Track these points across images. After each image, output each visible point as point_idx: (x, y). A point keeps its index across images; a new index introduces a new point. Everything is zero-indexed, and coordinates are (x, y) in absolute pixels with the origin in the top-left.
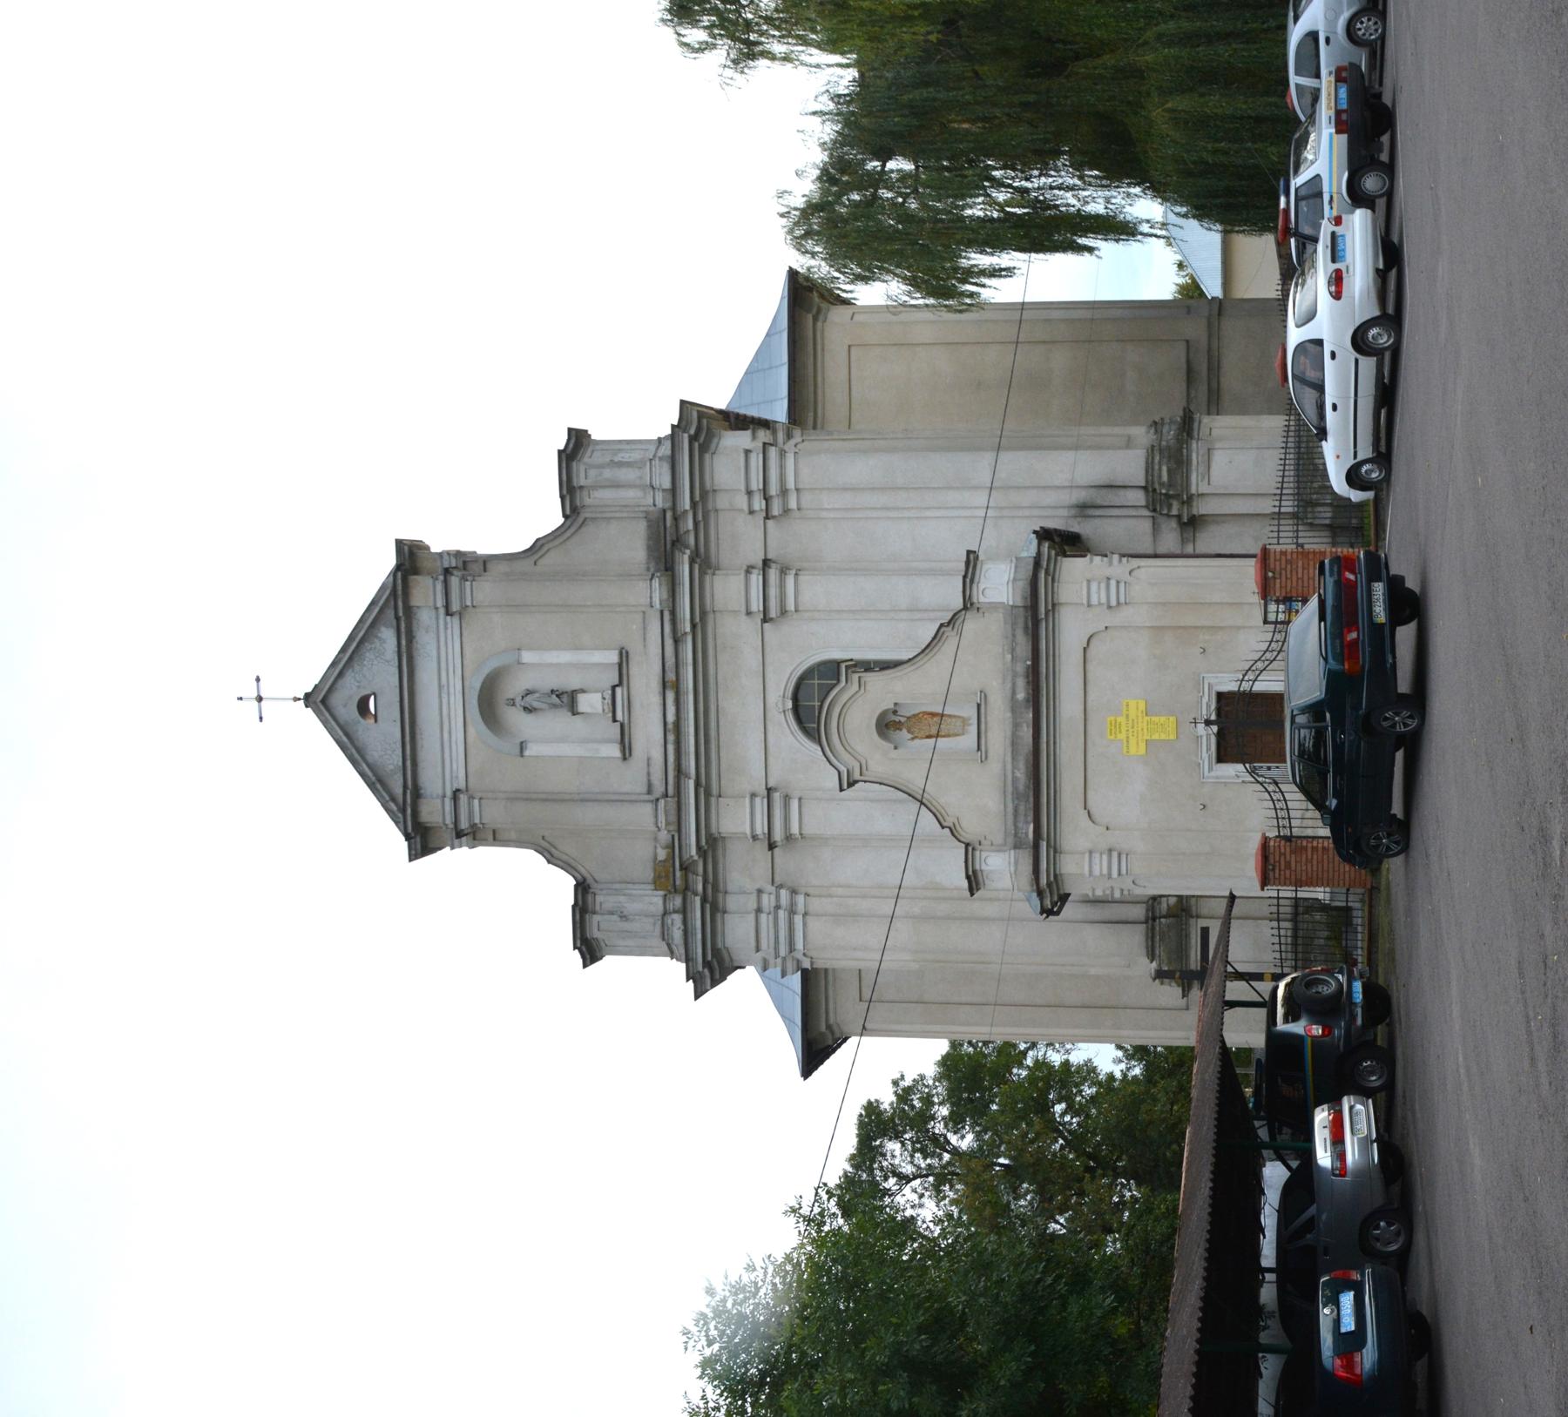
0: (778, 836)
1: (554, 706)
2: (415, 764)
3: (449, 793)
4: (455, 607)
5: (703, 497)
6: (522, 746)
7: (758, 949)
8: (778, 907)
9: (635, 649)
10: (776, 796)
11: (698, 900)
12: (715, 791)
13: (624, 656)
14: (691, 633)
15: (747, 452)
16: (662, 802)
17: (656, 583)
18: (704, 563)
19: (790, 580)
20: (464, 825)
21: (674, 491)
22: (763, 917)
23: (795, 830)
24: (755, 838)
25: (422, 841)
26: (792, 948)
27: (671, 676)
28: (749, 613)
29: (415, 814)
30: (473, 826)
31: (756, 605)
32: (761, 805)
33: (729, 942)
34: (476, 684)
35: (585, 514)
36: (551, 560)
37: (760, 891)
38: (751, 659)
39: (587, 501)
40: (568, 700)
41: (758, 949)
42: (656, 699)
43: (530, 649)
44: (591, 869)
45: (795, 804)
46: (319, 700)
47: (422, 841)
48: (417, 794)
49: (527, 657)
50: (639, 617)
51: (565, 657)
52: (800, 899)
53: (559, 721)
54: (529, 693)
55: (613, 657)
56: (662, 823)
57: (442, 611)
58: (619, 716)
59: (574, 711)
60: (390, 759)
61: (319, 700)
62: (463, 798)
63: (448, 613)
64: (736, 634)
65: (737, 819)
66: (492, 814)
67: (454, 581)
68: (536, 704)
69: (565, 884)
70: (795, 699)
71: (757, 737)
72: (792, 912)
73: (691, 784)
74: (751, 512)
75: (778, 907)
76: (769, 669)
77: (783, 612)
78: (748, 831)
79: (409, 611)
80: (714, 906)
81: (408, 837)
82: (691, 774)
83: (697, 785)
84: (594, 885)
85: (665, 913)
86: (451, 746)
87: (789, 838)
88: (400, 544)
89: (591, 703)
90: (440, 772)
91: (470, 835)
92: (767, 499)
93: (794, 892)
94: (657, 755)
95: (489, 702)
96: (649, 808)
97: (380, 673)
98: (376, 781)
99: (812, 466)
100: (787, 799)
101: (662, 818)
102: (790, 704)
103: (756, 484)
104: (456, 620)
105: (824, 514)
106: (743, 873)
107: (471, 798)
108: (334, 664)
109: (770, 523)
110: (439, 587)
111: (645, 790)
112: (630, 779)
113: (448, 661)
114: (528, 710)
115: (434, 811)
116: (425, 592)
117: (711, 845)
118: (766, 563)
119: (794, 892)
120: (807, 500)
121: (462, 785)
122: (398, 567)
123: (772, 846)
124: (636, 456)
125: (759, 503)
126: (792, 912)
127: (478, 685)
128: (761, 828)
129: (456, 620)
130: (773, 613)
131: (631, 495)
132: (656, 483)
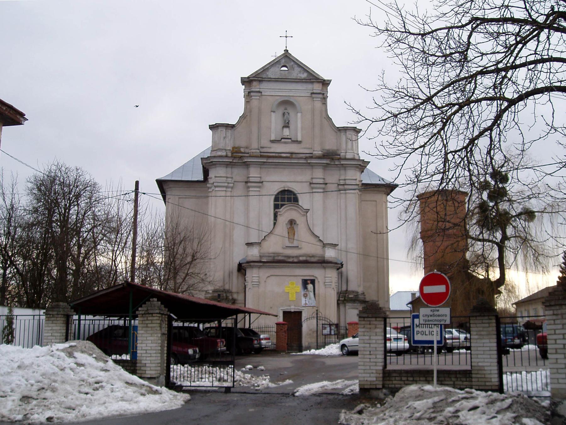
0: (249, 184)
1: (285, 121)
2: (269, 81)
3: (261, 90)
4: (313, 96)
5: (344, 167)
6: (274, 112)
7: (215, 177)
8: (228, 183)
9: (302, 145)
10: (260, 184)
11: (231, 161)
12: (262, 166)
13: (300, 142)
14: (307, 161)
15: (356, 180)
16: (258, 151)
17: (320, 152)
18: (326, 167)
19: (322, 191)
20: (252, 94)
21: (346, 159)
22: (225, 179)
23: (251, 189)
24: (249, 177)
25: (246, 81)
26: (215, 187)
27: (294, 156)
28: (312, 178)
29: (255, 80)
30: (251, 96)
31: (315, 181)
32: (258, 180)
33: (218, 168)
34: (292, 100)
35: (338, 133)
36: (325, 122)
37: (232, 178)
38: (299, 178)
39: (342, 134)
40: (286, 125)
41: (215, 177)
42: (287, 151)
43: (302, 115)
44: (239, 129)
45: (258, 189)
46: (286, 55)
47: (246, 81)
48: (260, 81)
49: (299, 115)
50: (310, 147)
51: (299, 125)
52: (230, 190)
53: (280, 124)
54: (289, 114)
55: (299, 139)
56: (252, 151)
57: (312, 91)
58: (283, 140)
59: (283, 127)
60: (271, 74)
61: (286, 55)
62: (260, 94)
63: (312, 93)
64: (305, 175)
65: (254, 173)
66: (255, 102)
67: (321, 96)
68: (286, 116)
69: (233, 121)
70: (288, 191)
71: (277, 180)
72: (227, 187)
73: (265, 161)
74: (340, 180)
75: (228, 183)
76: (296, 183)
77: (313, 188)
78: (250, 176)
79: (312, 82)
80: (228, 165)
81: (248, 78)
82: (268, 160)
83: (264, 162)
84: (233, 130)
85: (226, 150)
86: (272, 92)
87: (248, 187)
88: (330, 81)
89: (286, 132)
90: (267, 88)
91: (248, 96)
92: (343, 185)
93: (232, 188)
94: (272, 150)
95: (287, 103)
96: (257, 147)
97: (297, 73)
98: (265, 69)
99: (353, 197)
100: (259, 187)
101: (254, 151)
102: (286, 189)
103: (348, 182)
104: (310, 95)
105: (339, 200)
106: (238, 174)
107: (259, 96)
108: (297, 60)
109: (336, 185)
110: (319, 91)
111: (262, 146)
112: (265, 142)
113: (299, 92)
114: (284, 114)
115: (256, 87)
116: (317, 87)
117: (247, 165)
118: (326, 184)
119: (232, 188)
120: (343, 196)
121: (263, 94)
122: (324, 80)
123: (246, 182)
124: (354, 147)
125: (342, 182)
126: (227, 187)
127: (291, 100)
128: (251, 179)
129: (310, 95)
130: (312, 185)
131: (344, 146)
132: (347, 154)
